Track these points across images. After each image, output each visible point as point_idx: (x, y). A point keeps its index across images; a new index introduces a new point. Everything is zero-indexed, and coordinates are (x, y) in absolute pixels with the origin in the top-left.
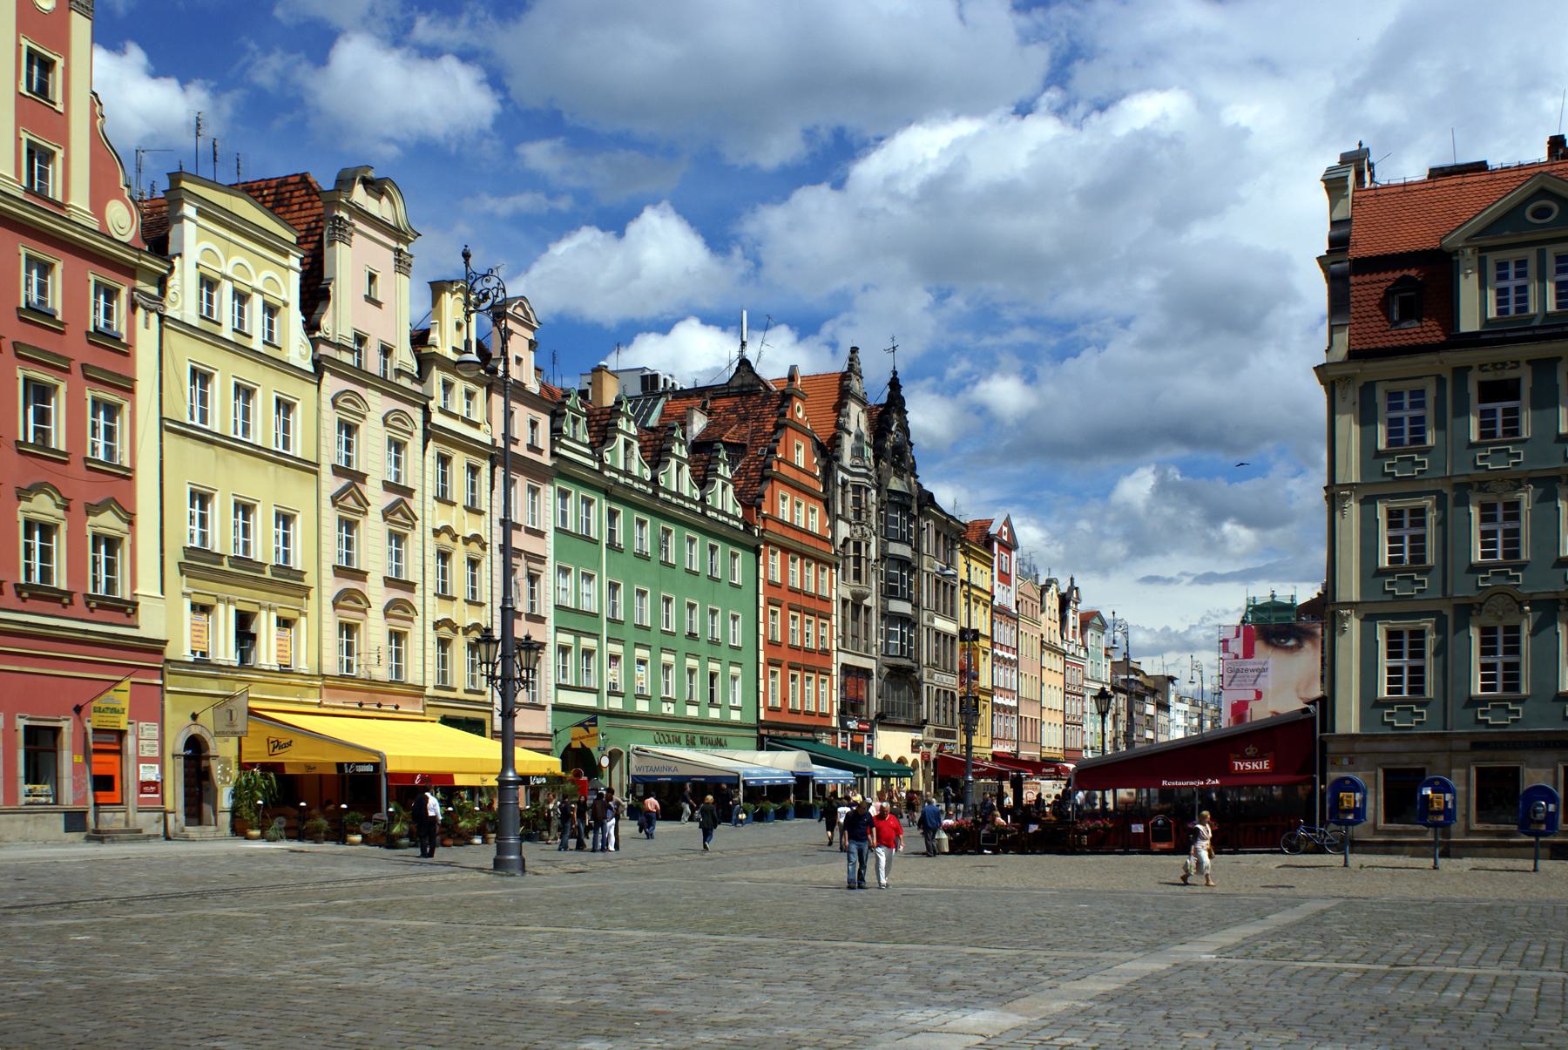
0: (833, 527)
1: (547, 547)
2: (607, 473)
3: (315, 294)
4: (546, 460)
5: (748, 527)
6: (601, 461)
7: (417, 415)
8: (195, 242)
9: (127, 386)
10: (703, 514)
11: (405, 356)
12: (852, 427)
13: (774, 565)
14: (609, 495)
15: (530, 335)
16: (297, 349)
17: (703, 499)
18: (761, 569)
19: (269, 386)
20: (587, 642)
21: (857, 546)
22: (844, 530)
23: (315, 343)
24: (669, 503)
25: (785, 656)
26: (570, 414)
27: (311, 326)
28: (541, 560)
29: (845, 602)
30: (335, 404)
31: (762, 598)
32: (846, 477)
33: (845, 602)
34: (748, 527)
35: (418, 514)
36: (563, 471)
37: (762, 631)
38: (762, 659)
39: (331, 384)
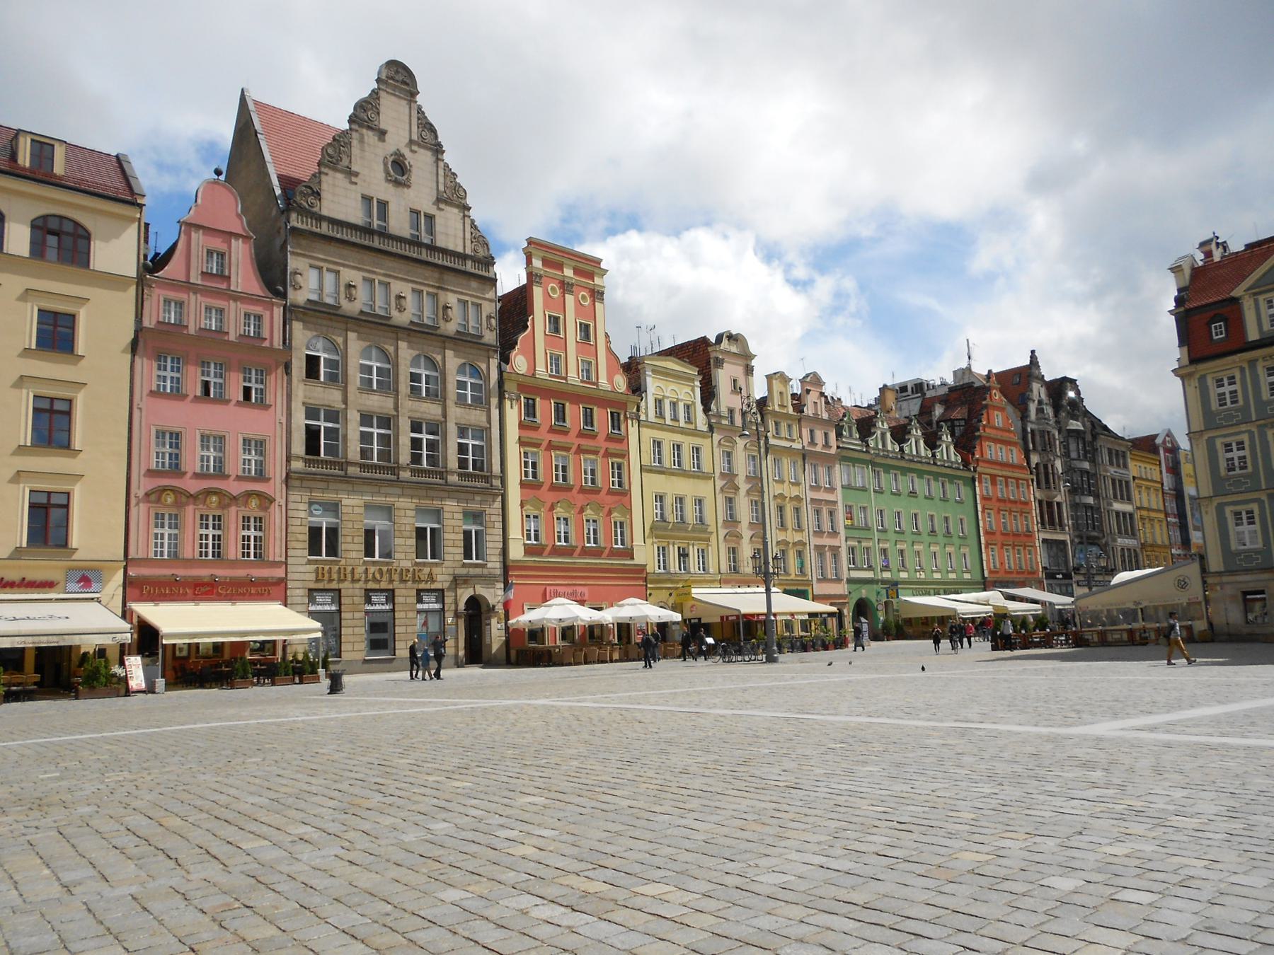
0: (1028, 458)
3: (708, 394)
6: (868, 446)
8: (653, 385)
9: (625, 455)
12: (1036, 398)
16: (701, 421)
19: (687, 442)
20: (864, 544)
21: (1046, 467)
22: (1035, 459)
27: (707, 410)
28: (835, 503)
29: (1040, 502)
32: (1034, 427)
36: (845, 457)
39: (716, 437)
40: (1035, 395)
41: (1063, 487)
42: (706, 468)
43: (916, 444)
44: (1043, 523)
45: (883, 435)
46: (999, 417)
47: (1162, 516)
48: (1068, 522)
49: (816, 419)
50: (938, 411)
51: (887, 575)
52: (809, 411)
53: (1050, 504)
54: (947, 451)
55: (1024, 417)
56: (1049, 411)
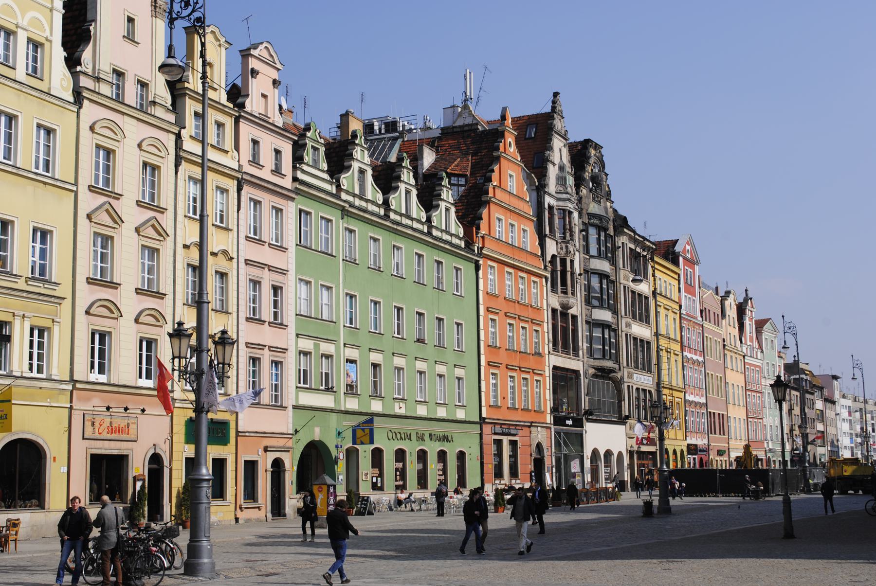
1: (289, 260)
2: (344, 196)
4: (287, 183)
5: (469, 244)
6: (338, 186)
7: (170, 141)
10: (429, 234)
11: (160, 90)
12: (557, 160)
13: (490, 276)
14: (345, 213)
15: (275, 75)
17: (429, 220)
18: (481, 281)
20: (327, 348)
21: (563, 261)
23: (75, 75)
24: (399, 224)
25: (503, 358)
26: (309, 143)
27: (72, 62)
28: (283, 272)
29: (554, 311)
30: (92, 128)
31: (482, 308)
32: (553, 202)
33: (554, 311)
34: (469, 244)
35: (170, 231)
37: (482, 337)
38: (483, 362)
39: (90, 112)
40: (555, 157)
41: (580, 293)
42: (62, 169)
43: (405, 197)
44: (555, 344)
45: (362, 172)
46: (510, 177)
47: (676, 347)
48: (583, 345)
49: (262, 122)
50: (429, 158)
51: (352, 404)
52: (253, 104)
53: (564, 315)
54: (446, 218)
55: (540, 189)
56: (570, 181)
